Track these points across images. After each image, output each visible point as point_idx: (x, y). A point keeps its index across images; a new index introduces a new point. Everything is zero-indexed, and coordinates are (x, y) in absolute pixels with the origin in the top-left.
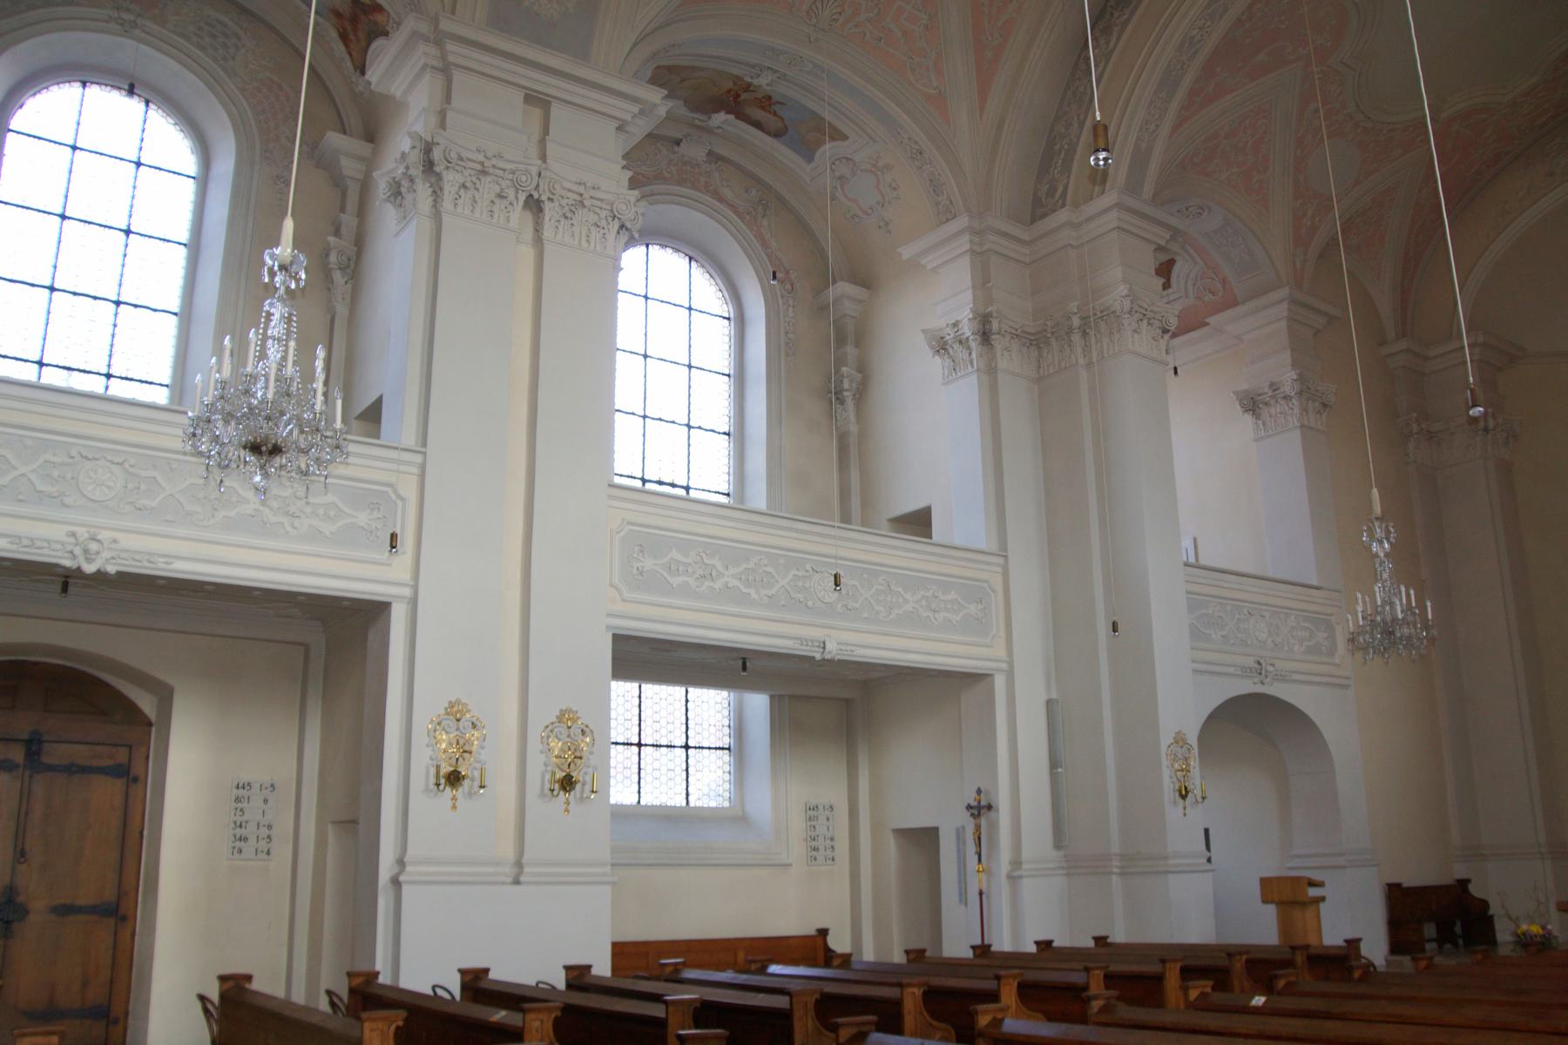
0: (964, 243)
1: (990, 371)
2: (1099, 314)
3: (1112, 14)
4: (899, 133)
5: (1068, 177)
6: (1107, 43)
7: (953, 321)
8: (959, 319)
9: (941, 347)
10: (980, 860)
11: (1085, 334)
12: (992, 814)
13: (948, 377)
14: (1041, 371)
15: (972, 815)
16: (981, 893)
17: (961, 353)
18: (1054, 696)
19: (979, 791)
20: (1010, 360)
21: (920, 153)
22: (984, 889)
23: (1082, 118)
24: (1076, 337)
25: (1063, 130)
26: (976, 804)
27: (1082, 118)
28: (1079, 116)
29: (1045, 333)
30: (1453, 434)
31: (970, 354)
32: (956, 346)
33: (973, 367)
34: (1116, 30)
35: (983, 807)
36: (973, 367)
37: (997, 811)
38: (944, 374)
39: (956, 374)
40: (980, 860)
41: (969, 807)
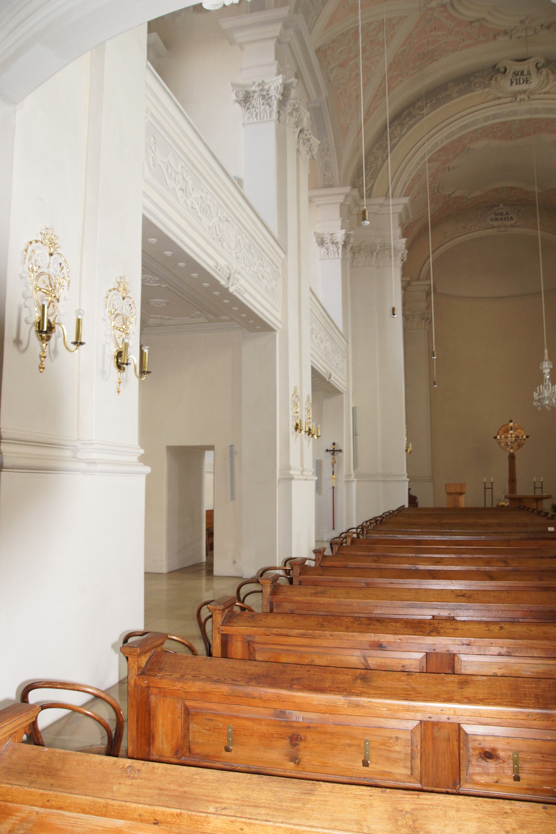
0: (341, 199)
1: (343, 259)
2: (387, 247)
3: (405, 118)
4: (323, 137)
5: (375, 182)
6: (401, 131)
7: (331, 232)
8: (335, 232)
9: (321, 242)
10: (333, 474)
11: (378, 253)
12: (340, 454)
13: (323, 257)
14: (354, 264)
15: (332, 454)
16: (333, 488)
17: (332, 248)
18: (354, 406)
19: (334, 444)
20: (349, 255)
21: (328, 150)
22: (335, 486)
23: (384, 158)
24: (375, 254)
25: (372, 160)
26: (332, 449)
27: (384, 158)
28: (382, 157)
29: (359, 248)
30: (414, 317)
31: (338, 249)
32: (330, 244)
33: (339, 256)
34: (406, 127)
35: (337, 451)
36: (339, 256)
37: (343, 453)
38: (320, 255)
39: (328, 256)
40: (333, 474)
41: (327, 451)
